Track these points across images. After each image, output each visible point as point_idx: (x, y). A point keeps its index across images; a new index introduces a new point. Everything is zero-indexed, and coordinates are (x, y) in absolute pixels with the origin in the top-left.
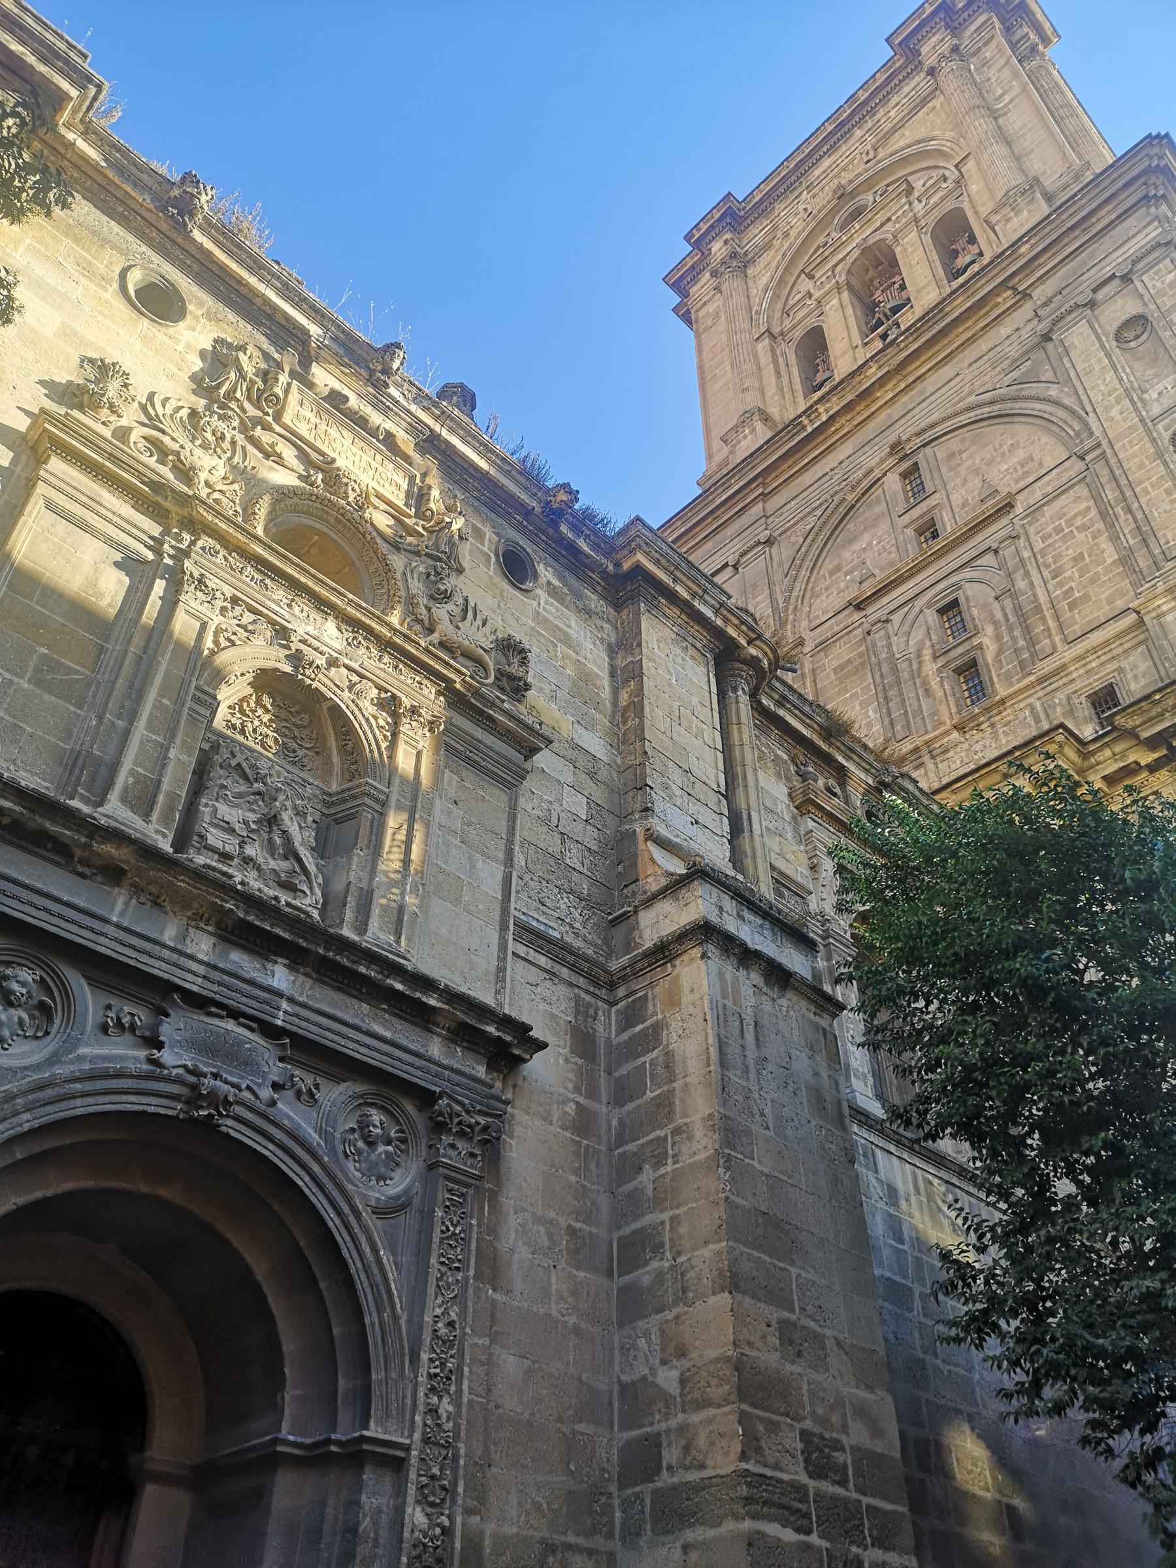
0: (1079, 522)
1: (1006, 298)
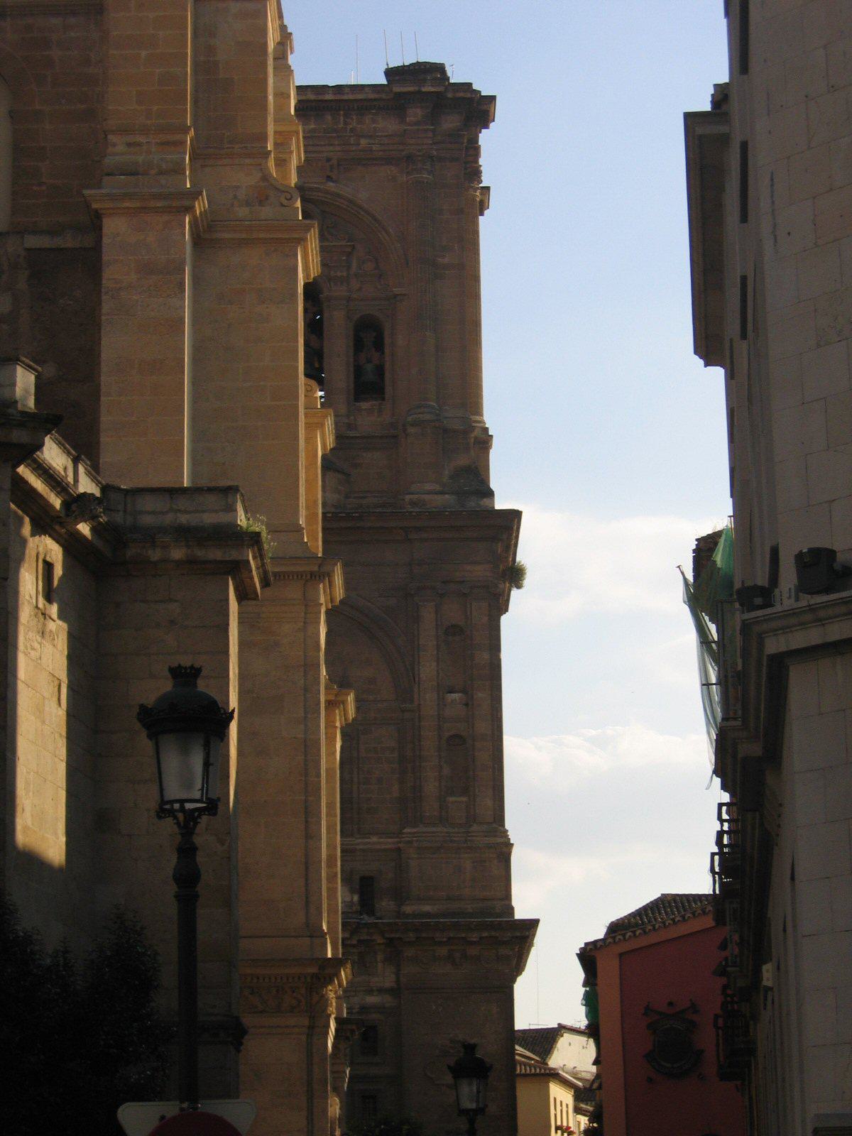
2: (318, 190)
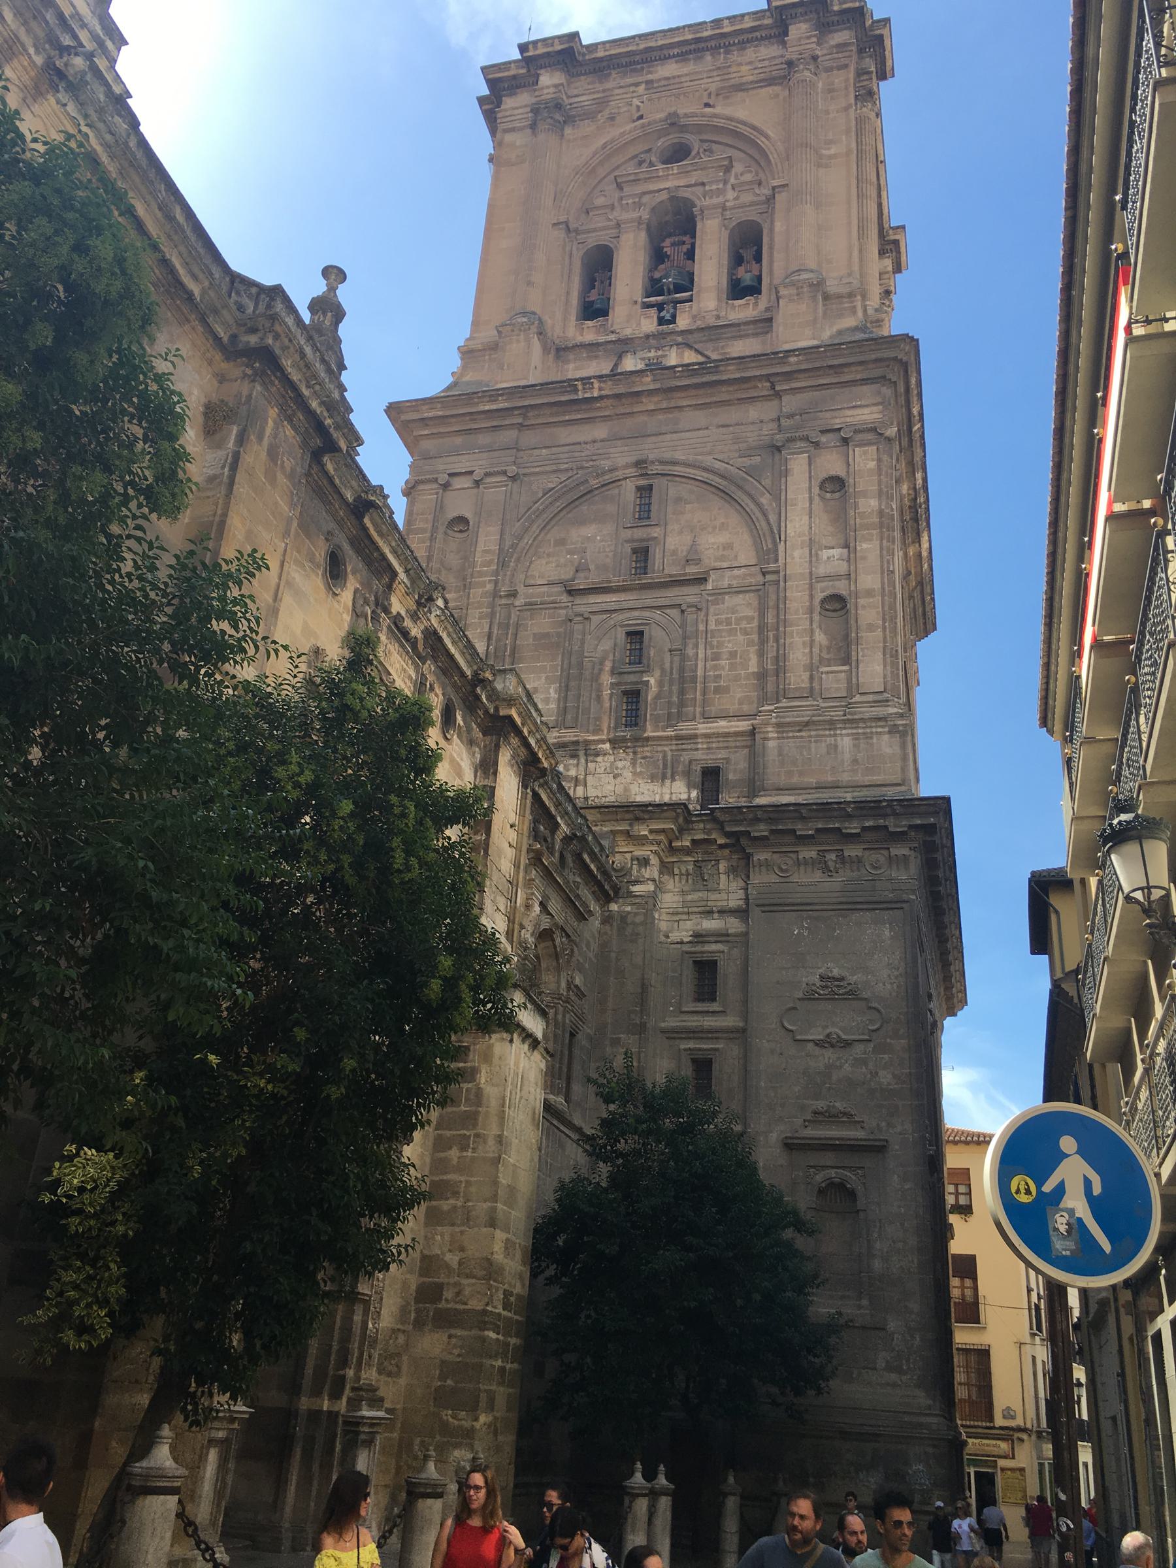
0: (744, 624)
1: (763, 388)
2: (694, 115)
